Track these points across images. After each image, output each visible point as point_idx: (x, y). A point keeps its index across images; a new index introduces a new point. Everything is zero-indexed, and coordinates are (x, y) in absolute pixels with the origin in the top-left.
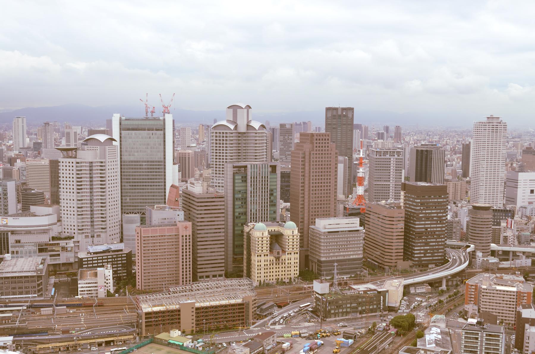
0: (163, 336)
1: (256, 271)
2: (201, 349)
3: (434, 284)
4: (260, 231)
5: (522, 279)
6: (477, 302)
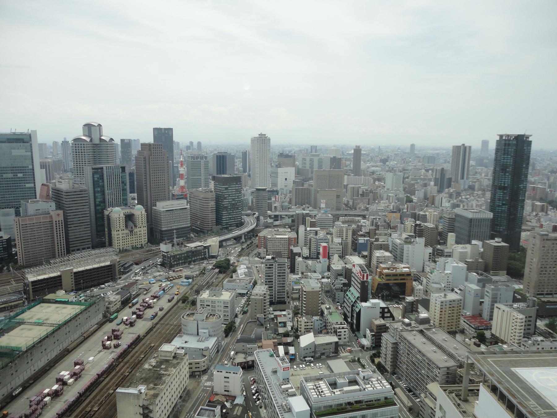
0: (50, 296)
1: (116, 242)
2: (83, 301)
3: (237, 239)
4: (117, 213)
5: (289, 230)
6: (266, 247)
